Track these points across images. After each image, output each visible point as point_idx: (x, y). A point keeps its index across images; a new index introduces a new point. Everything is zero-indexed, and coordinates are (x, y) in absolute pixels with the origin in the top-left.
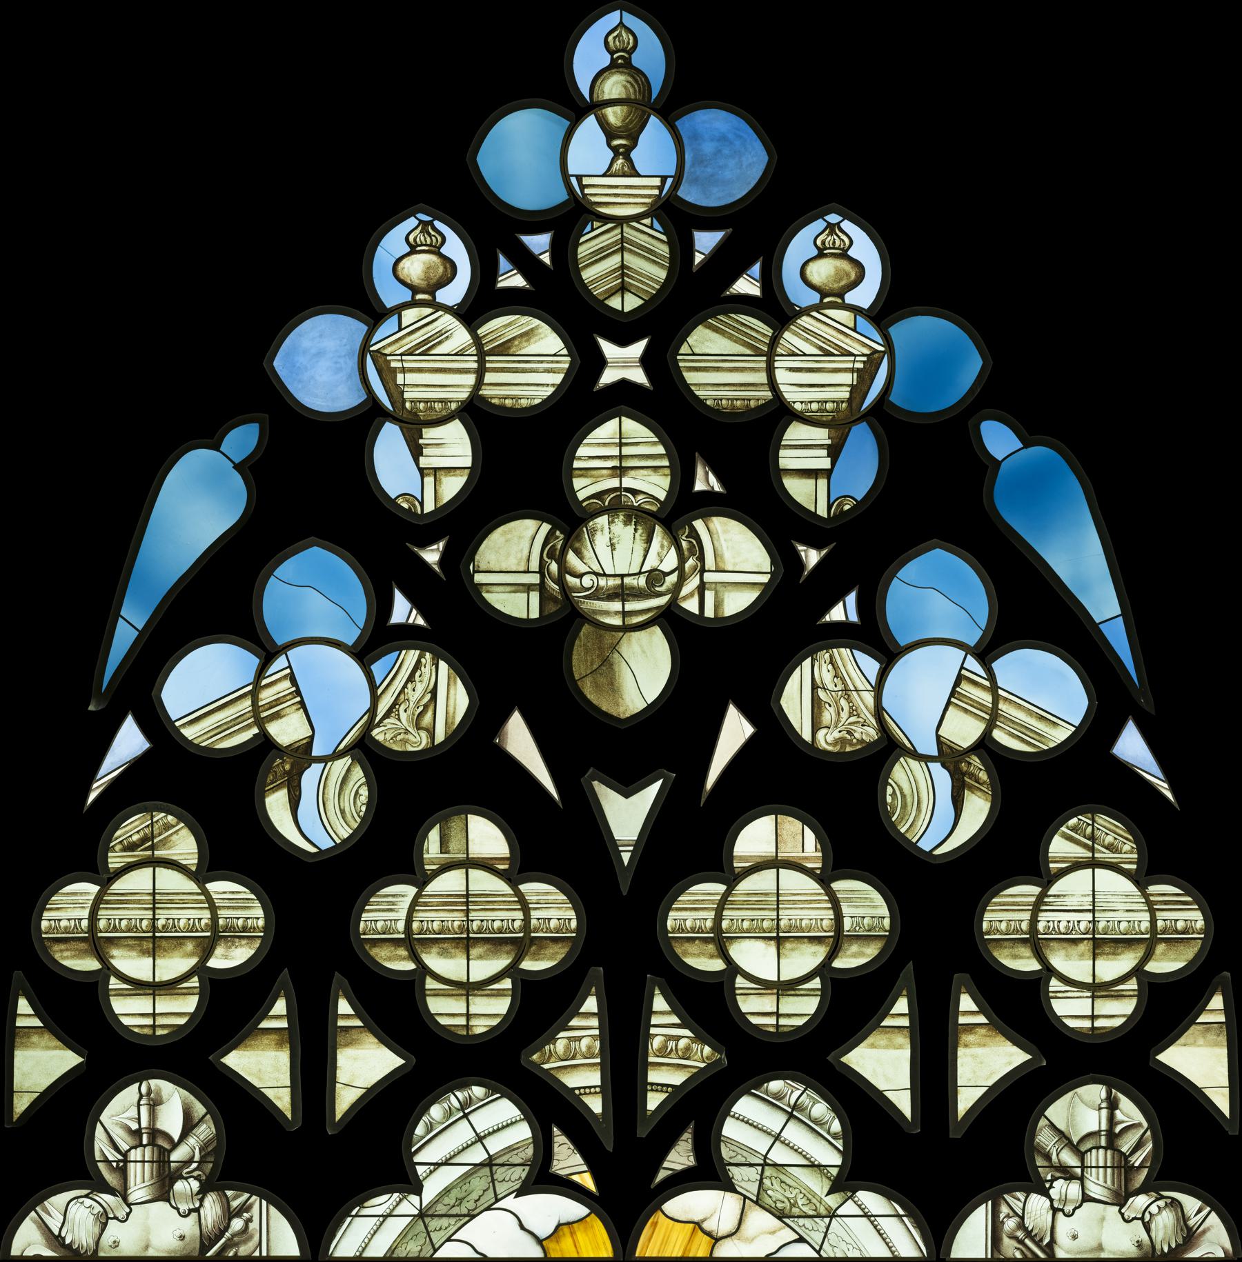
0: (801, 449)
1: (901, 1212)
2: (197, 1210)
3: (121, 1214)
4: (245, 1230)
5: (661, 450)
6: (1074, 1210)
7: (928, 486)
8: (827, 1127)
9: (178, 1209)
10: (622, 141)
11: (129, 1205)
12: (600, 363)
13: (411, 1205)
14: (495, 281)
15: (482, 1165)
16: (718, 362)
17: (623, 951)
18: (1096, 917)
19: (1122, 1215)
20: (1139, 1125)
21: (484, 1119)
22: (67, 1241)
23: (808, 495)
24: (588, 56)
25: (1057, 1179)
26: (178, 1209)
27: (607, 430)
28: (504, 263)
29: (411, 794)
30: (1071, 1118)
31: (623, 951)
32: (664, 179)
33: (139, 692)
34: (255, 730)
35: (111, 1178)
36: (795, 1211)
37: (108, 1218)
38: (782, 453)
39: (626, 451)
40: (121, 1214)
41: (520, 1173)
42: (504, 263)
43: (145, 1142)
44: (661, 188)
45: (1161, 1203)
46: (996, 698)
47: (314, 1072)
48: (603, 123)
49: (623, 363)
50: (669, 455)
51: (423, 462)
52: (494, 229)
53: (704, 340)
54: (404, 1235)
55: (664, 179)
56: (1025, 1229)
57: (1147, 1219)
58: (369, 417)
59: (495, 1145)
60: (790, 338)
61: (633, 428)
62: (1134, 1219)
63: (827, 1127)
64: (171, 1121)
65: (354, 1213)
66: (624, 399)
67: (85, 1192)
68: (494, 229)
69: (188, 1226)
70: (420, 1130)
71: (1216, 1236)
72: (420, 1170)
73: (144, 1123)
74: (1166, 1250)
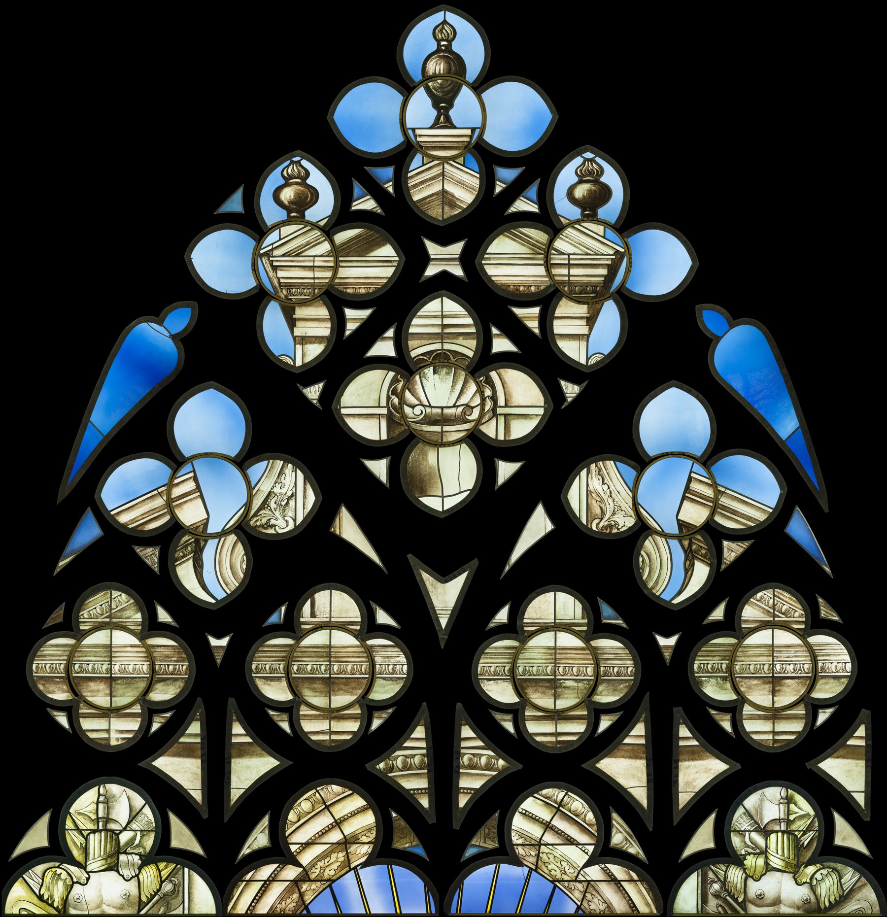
0: (569, 318)
1: (635, 877)
2: (137, 876)
3: (83, 880)
4: (173, 892)
5: (470, 321)
6: (761, 876)
7: (662, 346)
8: (582, 816)
9: (123, 876)
10: (443, 103)
11: (88, 873)
12: (426, 259)
13: (291, 872)
14: (350, 205)
15: (338, 843)
16: (509, 260)
17: (442, 685)
18: (781, 661)
19: (796, 880)
20: (808, 815)
21: (340, 811)
22: (46, 897)
23: (573, 351)
24: (418, 43)
25: (749, 854)
26: (123, 876)
27: (433, 306)
28: (357, 188)
29: (284, 569)
30: (759, 809)
31: (442, 685)
32: (473, 130)
33: (87, 495)
34: (167, 518)
35: (77, 854)
36: (566, 878)
37: (73, 883)
38: (556, 323)
39: (447, 321)
40: (83, 880)
41: (366, 849)
42: (357, 188)
43: (100, 828)
44: (471, 137)
45: (824, 872)
46: (718, 493)
47: (216, 774)
48: (428, 90)
49: (443, 258)
50: (475, 324)
51: (298, 332)
52: (347, 166)
53: (502, 245)
54: (282, 897)
55: (473, 130)
56: (726, 890)
57: (814, 882)
58: (259, 297)
59: (349, 828)
60: (559, 244)
61: (451, 306)
62: (804, 883)
63: (582, 816)
64: (121, 814)
65: (248, 877)
66: (444, 284)
67: (57, 864)
68: (347, 166)
69: (132, 887)
70: (292, 816)
71: (868, 897)
72: (293, 848)
73: (101, 815)
74: (827, 904)
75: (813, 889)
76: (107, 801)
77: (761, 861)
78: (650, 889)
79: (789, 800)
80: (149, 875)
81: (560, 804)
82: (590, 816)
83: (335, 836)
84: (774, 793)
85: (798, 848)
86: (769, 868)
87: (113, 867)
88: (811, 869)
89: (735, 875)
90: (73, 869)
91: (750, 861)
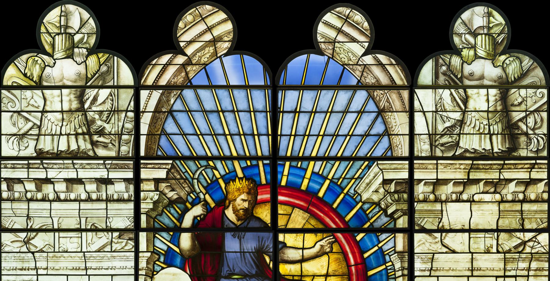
1: (394, 62)
2: (85, 61)
6: (472, 62)
8: (361, 24)
9: (76, 62)
11: (54, 60)
13: (180, 59)
15: (210, 41)
19: (493, 64)
20: (501, 24)
21: (211, 21)
22: (28, 75)
25: (465, 48)
26: (76, 62)
30: (471, 20)
35: (48, 48)
36: (351, 63)
37: (46, 66)
40: (52, 64)
41: (227, 45)
43: (62, 32)
45: (511, 59)
54: (175, 75)
56: (450, 70)
57: (505, 65)
59: (217, 32)
62: (499, 66)
63: (361, 24)
64: (75, 23)
65: (154, 62)
67: (35, 54)
69: (82, 68)
70: (181, 25)
72: (182, 44)
73: (62, 23)
74: (513, 79)
75: (504, 69)
76: (66, 15)
77: (472, 52)
78: (403, 70)
79: (489, 15)
80: (92, 61)
81: (347, 17)
82: (366, 25)
83: (208, 37)
84: (480, 10)
85: (495, 44)
86: (477, 57)
87: (70, 56)
88: (503, 58)
89: (456, 61)
90: (45, 57)
91: (465, 52)
